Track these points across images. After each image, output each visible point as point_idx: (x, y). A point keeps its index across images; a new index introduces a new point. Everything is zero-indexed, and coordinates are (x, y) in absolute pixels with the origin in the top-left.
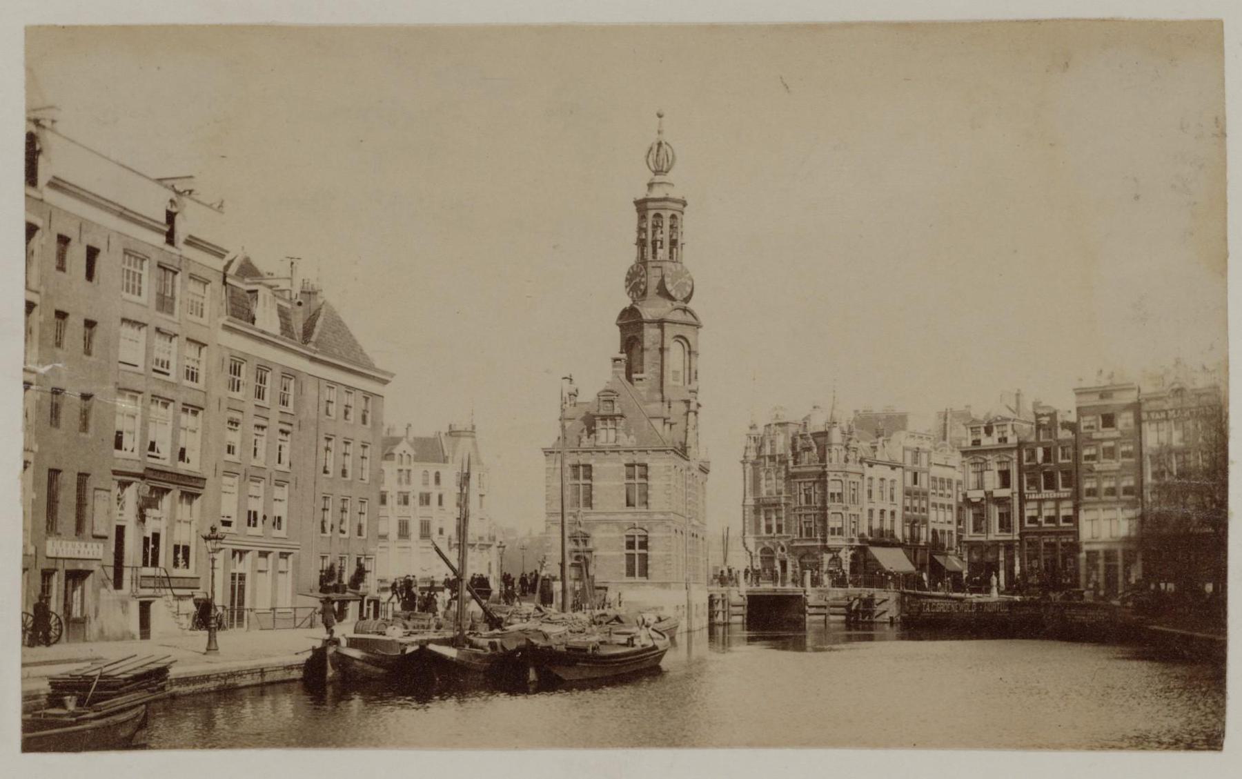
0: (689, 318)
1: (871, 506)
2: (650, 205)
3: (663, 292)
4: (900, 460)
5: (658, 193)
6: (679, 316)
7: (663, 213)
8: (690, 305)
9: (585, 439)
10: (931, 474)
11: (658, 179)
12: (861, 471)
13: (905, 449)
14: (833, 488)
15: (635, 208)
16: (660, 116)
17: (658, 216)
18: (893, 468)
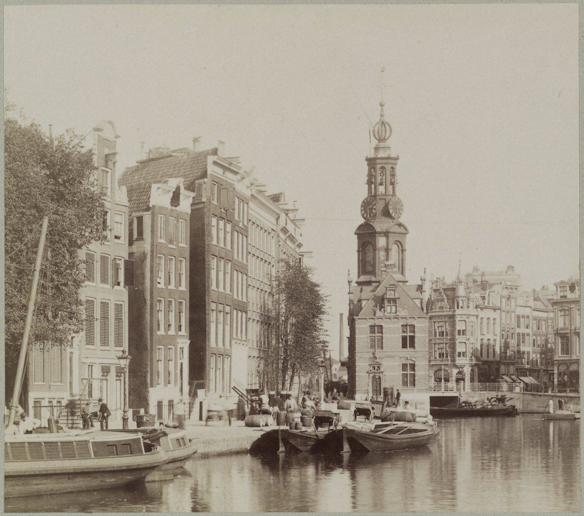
0: (402, 230)
1: (482, 337)
2: (378, 161)
3: (386, 213)
4: (498, 305)
5: (382, 154)
6: (397, 229)
7: (386, 166)
8: (401, 220)
9: (378, 311)
10: (517, 313)
11: (382, 145)
12: (476, 313)
13: (502, 297)
14: (460, 326)
15: (366, 163)
16: (382, 105)
17: (383, 168)
18: (495, 310)
